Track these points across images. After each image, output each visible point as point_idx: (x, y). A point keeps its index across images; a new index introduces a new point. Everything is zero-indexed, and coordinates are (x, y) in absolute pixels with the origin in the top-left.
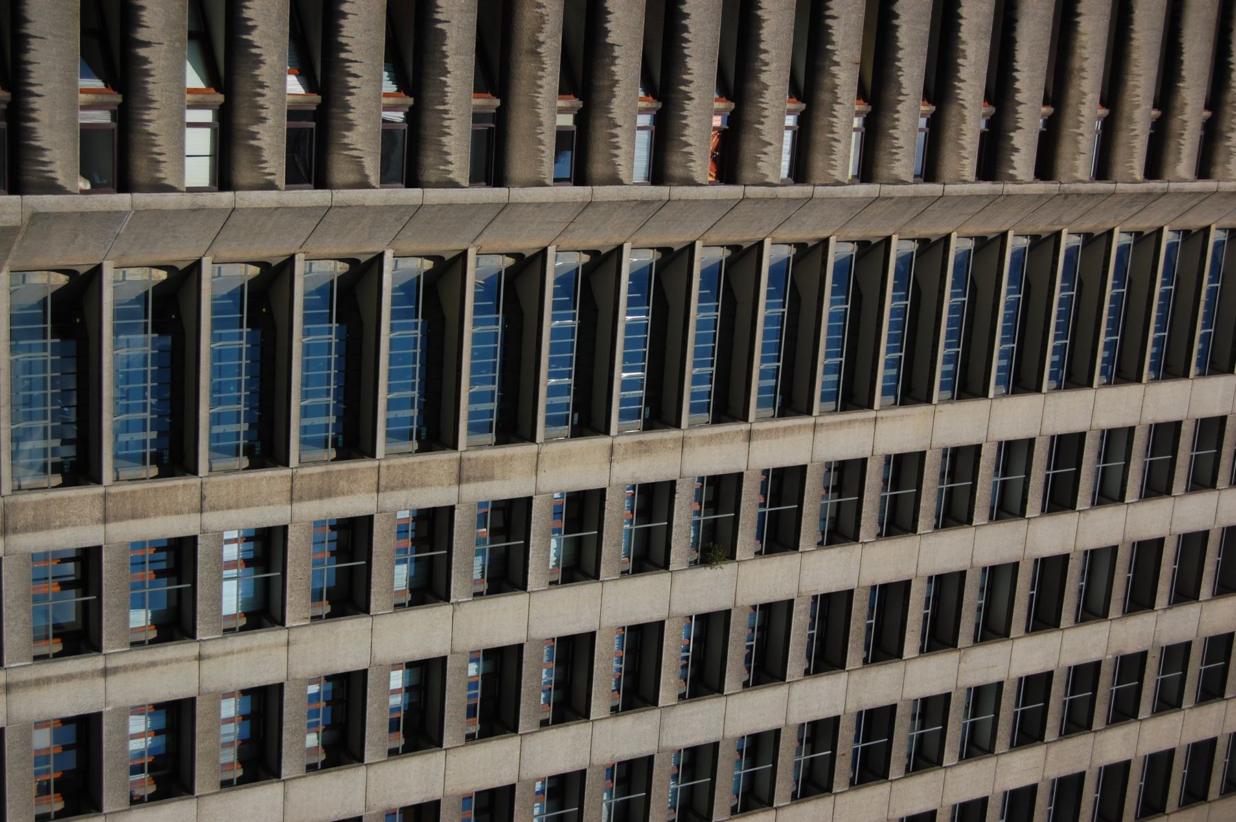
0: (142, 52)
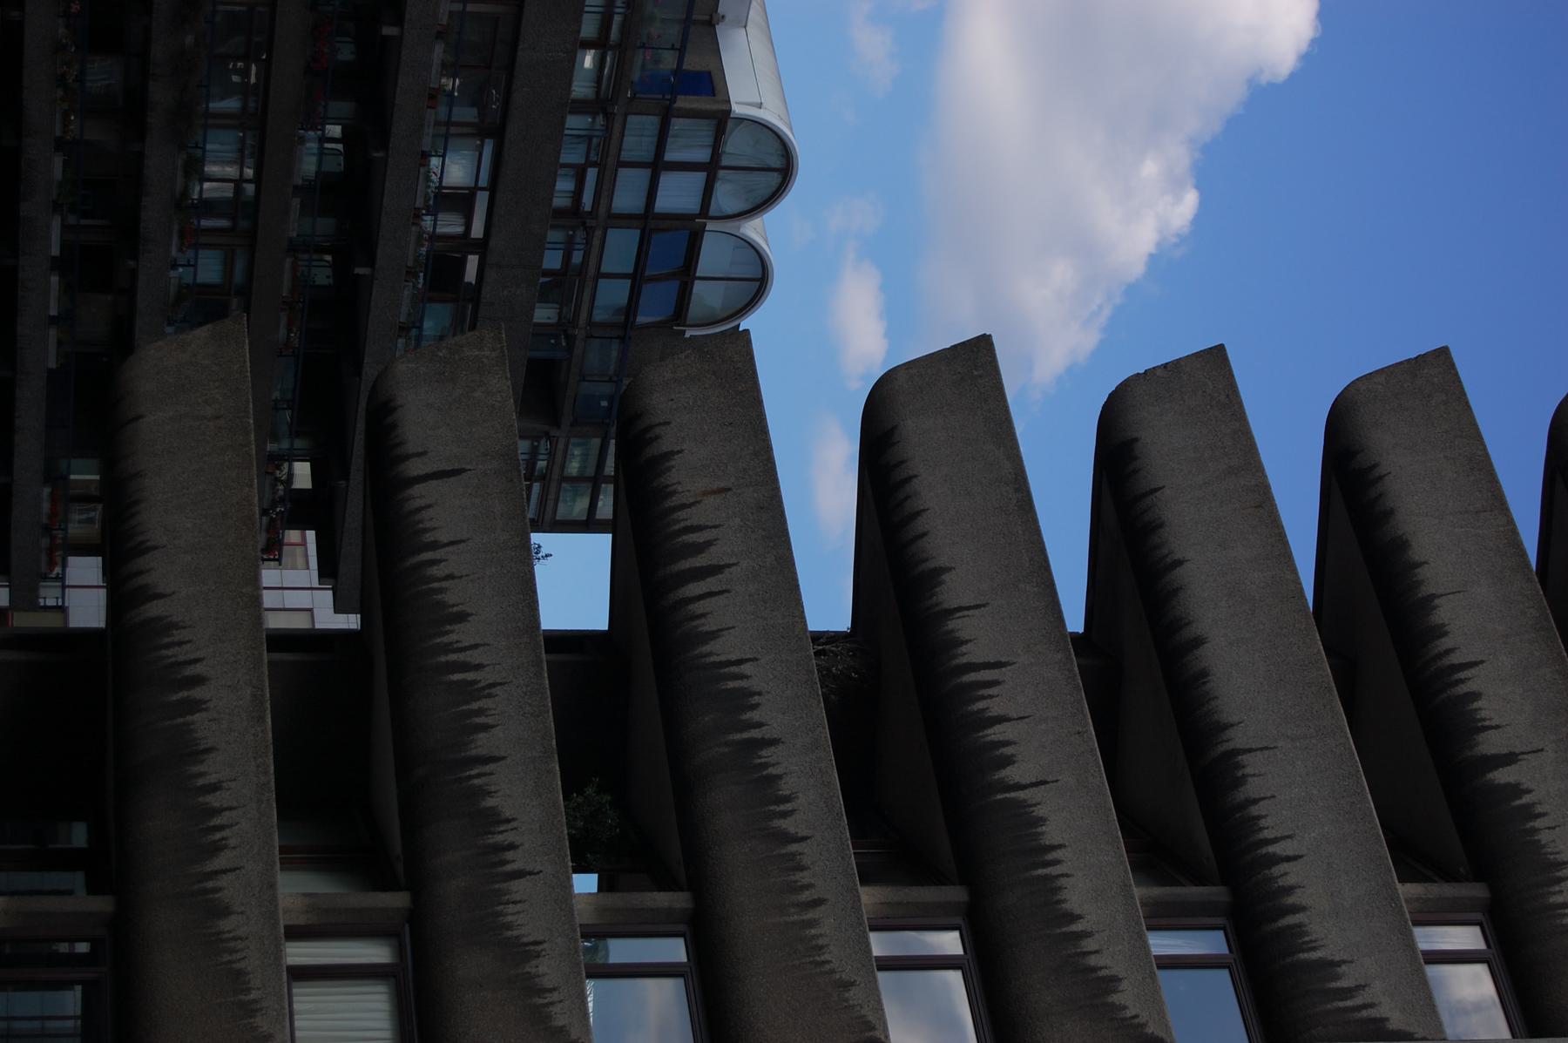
0: (1502, 776)
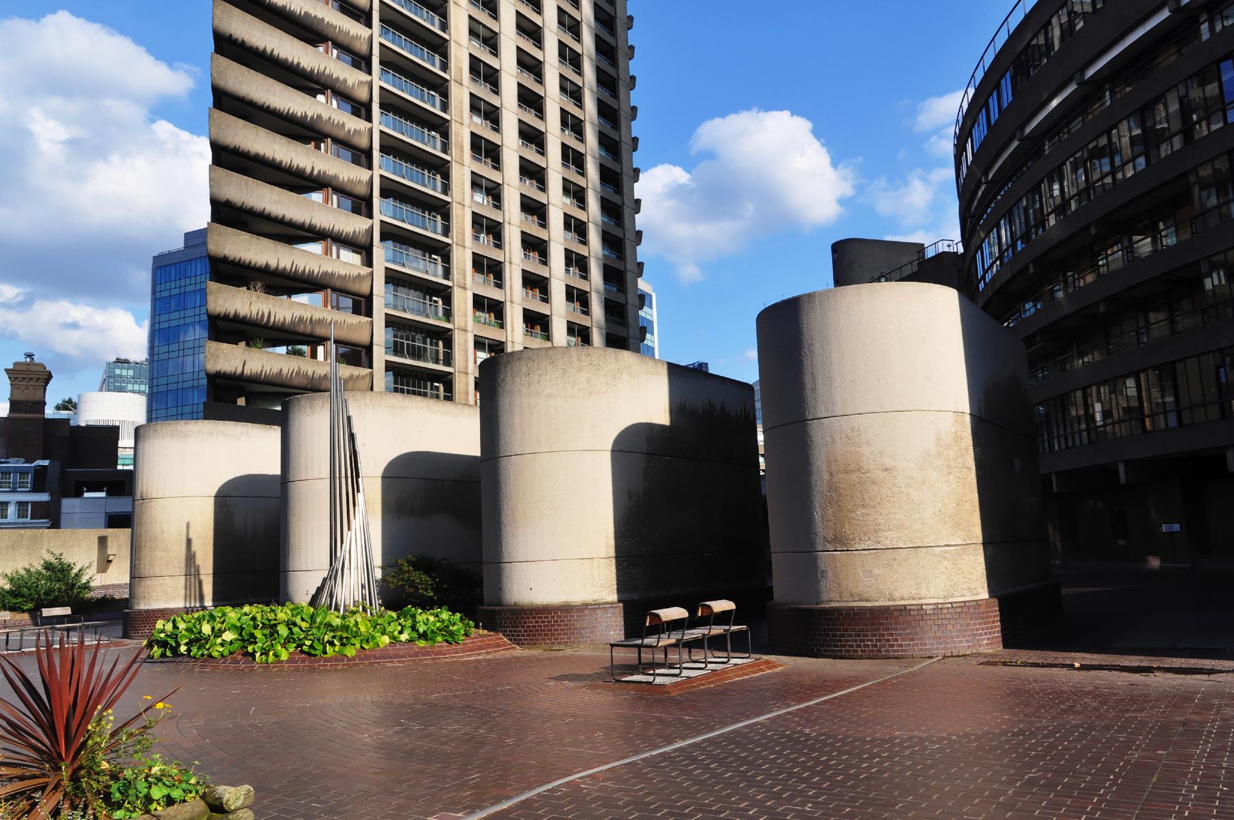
0: (316, 172)
